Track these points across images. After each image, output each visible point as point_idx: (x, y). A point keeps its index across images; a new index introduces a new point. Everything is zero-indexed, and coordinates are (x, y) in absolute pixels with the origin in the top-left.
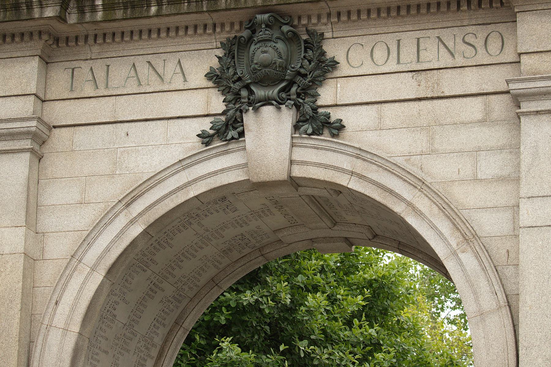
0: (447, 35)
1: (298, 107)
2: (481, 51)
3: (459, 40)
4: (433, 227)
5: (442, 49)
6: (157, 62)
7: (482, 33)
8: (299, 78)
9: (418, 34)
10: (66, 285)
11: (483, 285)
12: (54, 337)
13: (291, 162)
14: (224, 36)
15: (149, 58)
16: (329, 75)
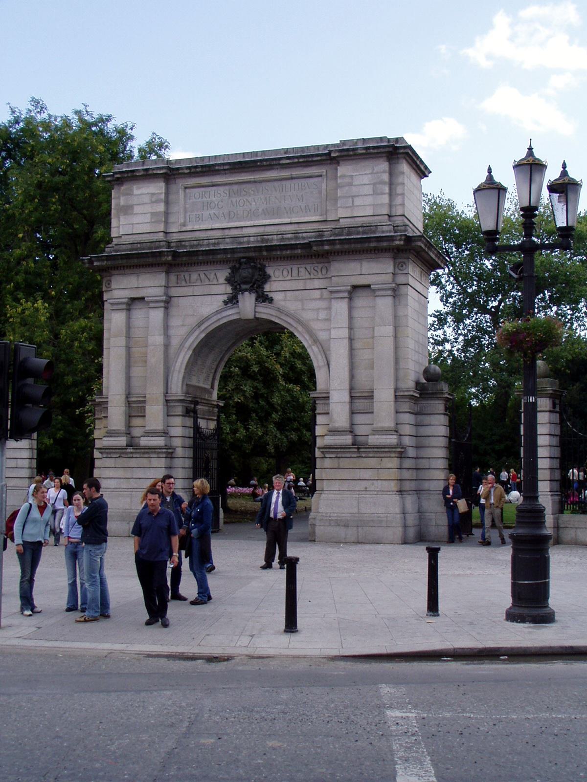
0: (308, 267)
2: (320, 273)
6: (207, 273)
7: (320, 266)
8: (257, 282)
9: (299, 266)
10: (179, 354)
11: (320, 357)
12: (175, 375)
13: (255, 312)
15: (204, 272)
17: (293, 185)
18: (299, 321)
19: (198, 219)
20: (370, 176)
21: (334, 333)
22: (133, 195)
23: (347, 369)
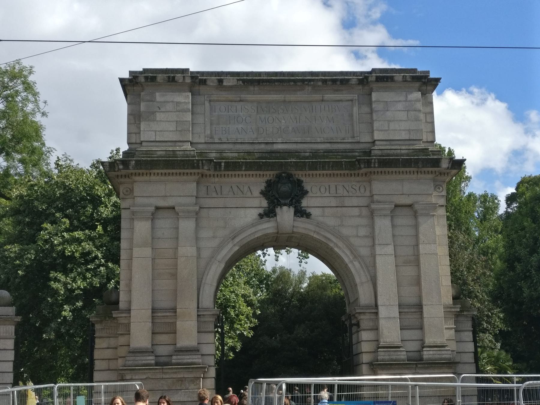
1: (295, 207)
2: (358, 191)
3: (350, 187)
4: (344, 252)
5: (345, 190)
11: (362, 272)
14: (266, 179)
16: (305, 196)
17: (323, 107)
18: (340, 237)
19: (224, 132)
20: (404, 103)
21: (378, 250)
22: (154, 101)
23: (395, 285)
